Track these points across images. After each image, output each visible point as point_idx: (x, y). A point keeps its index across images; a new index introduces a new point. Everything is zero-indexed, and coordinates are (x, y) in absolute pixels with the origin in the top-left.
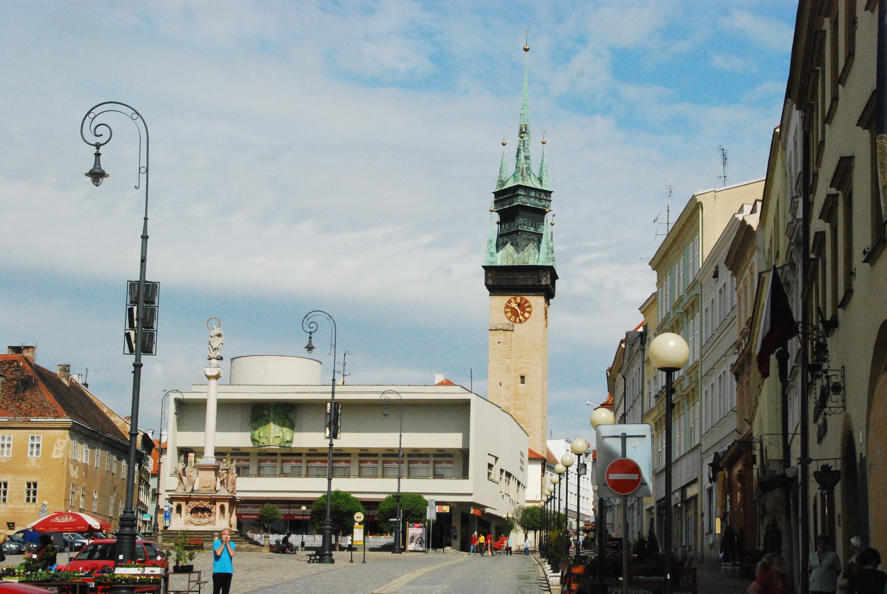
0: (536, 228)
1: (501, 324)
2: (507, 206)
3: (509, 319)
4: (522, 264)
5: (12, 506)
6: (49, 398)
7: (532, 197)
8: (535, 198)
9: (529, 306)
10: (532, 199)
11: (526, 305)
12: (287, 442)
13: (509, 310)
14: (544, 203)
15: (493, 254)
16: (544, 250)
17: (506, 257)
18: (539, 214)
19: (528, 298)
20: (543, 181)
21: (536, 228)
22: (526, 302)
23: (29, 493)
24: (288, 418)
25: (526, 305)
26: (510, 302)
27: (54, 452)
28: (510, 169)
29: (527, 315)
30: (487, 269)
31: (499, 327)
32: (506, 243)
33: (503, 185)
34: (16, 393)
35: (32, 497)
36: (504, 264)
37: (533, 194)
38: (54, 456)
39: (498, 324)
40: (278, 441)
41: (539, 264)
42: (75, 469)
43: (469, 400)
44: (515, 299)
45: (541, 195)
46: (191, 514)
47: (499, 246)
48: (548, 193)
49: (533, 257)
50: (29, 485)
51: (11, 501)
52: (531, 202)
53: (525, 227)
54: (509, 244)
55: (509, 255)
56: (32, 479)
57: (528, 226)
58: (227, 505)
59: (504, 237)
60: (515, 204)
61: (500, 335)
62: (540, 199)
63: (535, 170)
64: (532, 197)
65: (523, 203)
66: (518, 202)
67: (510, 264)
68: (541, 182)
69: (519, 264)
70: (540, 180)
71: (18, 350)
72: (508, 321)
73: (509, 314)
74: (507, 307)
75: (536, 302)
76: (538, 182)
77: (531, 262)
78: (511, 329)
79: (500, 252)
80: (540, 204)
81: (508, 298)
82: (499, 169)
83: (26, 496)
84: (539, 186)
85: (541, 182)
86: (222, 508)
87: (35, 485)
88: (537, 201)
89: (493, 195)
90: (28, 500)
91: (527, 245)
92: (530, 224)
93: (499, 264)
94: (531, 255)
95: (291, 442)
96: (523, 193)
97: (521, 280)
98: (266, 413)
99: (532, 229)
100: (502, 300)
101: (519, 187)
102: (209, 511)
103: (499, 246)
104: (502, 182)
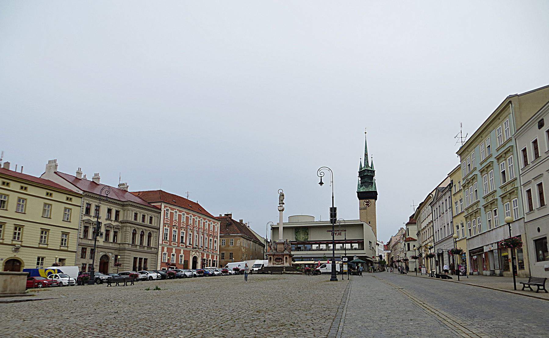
5: (226, 260)
6: (236, 228)
8: (370, 173)
12: (306, 239)
19: (370, 200)
21: (371, 181)
22: (370, 201)
23: (230, 256)
24: (306, 232)
28: (363, 166)
33: (361, 169)
34: (226, 227)
35: (231, 257)
38: (237, 245)
40: (303, 239)
42: (243, 249)
50: (230, 253)
58: (288, 257)
61: (363, 211)
62: (372, 173)
63: (370, 165)
67: (364, 191)
70: (371, 168)
71: (227, 215)
77: (370, 190)
80: (372, 174)
83: (229, 257)
84: (371, 170)
87: (232, 254)
93: (361, 191)
95: (307, 239)
98: (299, 230)
99: (370, 181)
101: (366, 170)
103: (361, 186)
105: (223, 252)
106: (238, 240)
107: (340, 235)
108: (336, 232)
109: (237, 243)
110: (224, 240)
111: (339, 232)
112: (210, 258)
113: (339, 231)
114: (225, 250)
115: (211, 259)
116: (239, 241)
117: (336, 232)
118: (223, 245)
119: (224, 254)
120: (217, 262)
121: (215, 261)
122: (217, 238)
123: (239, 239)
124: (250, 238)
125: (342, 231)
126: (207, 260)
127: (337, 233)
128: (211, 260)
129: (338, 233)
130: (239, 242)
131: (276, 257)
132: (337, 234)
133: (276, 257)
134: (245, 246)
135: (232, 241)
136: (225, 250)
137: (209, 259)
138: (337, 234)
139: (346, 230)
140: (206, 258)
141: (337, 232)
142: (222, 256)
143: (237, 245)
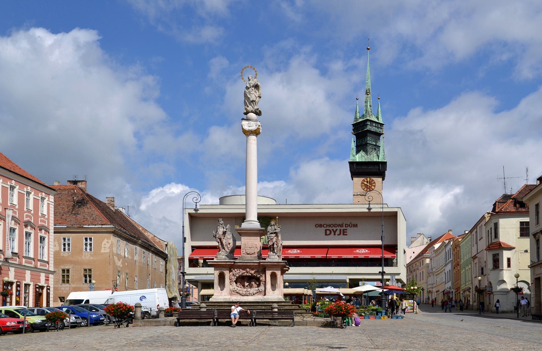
0: (376, 142)
1: (359, 192)
2: (360, 131)
3: (364, 189)
4: (370, 161)
7: (374, 126)
8: (375, 126)
9: (374, 183)
10: (374, 127)
11: (372, 182)
13: (363, 185)
14: (380, 130)
15: (354, 155)
16: (382, 154)
17: (360, 157)
18: (378, 135)
20: (379, 119)
22: (373, 180)
25: (372, 182)
26: (364, 180)
27: (103, 248)
29: (373, 187)
30: (351, 164)
31: (359, 194)
32: (360, 151)
36: (361, 161)
37: (374, 125)
38: (103, 251)
39: (358, 192)
41: (380, 161)
43: (397, 212)
44: (367, 179)
45: (378, 125)
46: (236, 283)
47: (358, 152)
48: (382, 125)
49: (373, 158)
51: (73, 283)
52: (373, 129)
53: (371, 142)
54: (362, 151)
55: (362, 156)
56: (87, 267)
57: (372, 141)
59: (359, 148)
60: (365, 129)
62: (378, 128)
64: (374, 126)
65: (369, 129)
66: (369, 128)
67: (364, 160)
68: (378, 119)
69: (369, 161)
72: (363, 191)
73: (364, 187)
74: (362, 183)
75: (378, 180)
76: (376, 119)
77: (375, 159)
78: (365, 195)
79: (358, 155)
80: (378, 130)
81: (364, 178)
82: (355, 112)
84: (377, 121)
85: (378, 119)
86: (274, 277)
88: (376, 129)
89: (352, 126)
90: (86, 281)
91: (372, 152)
92: (373, 141)
93: (358, 160)
94: (375, 156)
96: (370, 124)
97: (371, 168)
99: (374, 143)
100: (358, 180)
101: (368, 120)
102: (258, 281)
103: (358, 152)
104: (356, 119)
105: (67, 267)
106: (106, 240)
107: (344, 234)
108: (335, 229)
109: (103, 246)
110: (69, 240)
111: (342, 228)
112: (28, 280)
113: (341, 226)
114: (71, 262)
115: (32, 284)
116: (108, 242)
117: (335, 229)
118: (64, 250)
119: (68, 271)
120: (48, 289)
121: (42, 288)
122: (47, 231)
123: (108, 238)
124: (135, 237)
125: (349, 226)
126: (18, 286)
127: (337, 230)
128: (29, 285)
129: (340, 230)
130: (108, 245)
131: (238, 272)
132: (338, 232)
133: (238, 272)
134: (123, 254)
135: (89, 242)
136: (71, 262)
137: (24, 282)
138: (338, 232)
139: (357, 225)
140: (15, 281)
141: (339, 228)
142: (63, 276)
143: (103, 251)
